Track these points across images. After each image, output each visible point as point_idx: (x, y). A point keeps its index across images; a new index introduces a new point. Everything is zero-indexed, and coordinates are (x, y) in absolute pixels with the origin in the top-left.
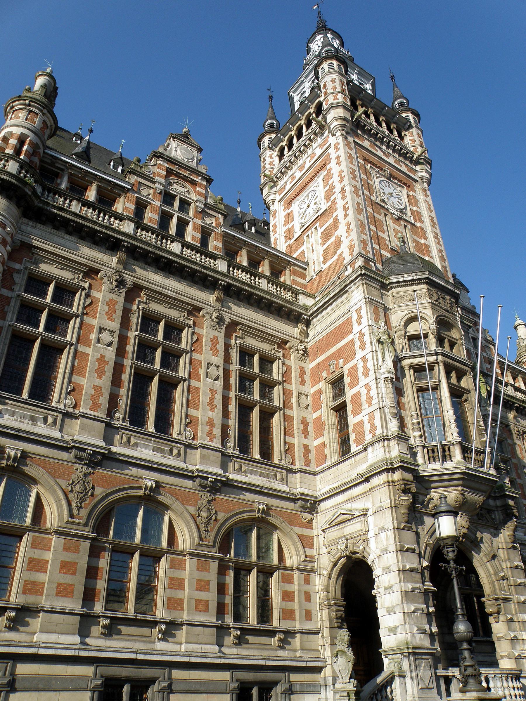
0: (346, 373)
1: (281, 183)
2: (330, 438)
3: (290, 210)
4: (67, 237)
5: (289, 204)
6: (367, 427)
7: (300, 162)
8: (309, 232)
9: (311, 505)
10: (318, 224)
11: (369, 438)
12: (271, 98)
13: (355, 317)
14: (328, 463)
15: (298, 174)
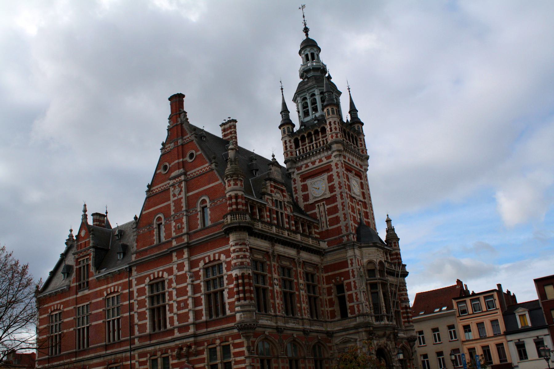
0: (345, 284)
1: (299, 164)
2: (337, 308)
3: (305, 183)
4: (259, 239)
5: (305, 178)
6: (356, 309)
7: (313, 159)
8: (319, 204)
9: (330, 334)
10: (324, 202)
11: (357, 313)
12: (282, 89)
13: (349, 262)
14: (336, 319)
15: (311, 166)
